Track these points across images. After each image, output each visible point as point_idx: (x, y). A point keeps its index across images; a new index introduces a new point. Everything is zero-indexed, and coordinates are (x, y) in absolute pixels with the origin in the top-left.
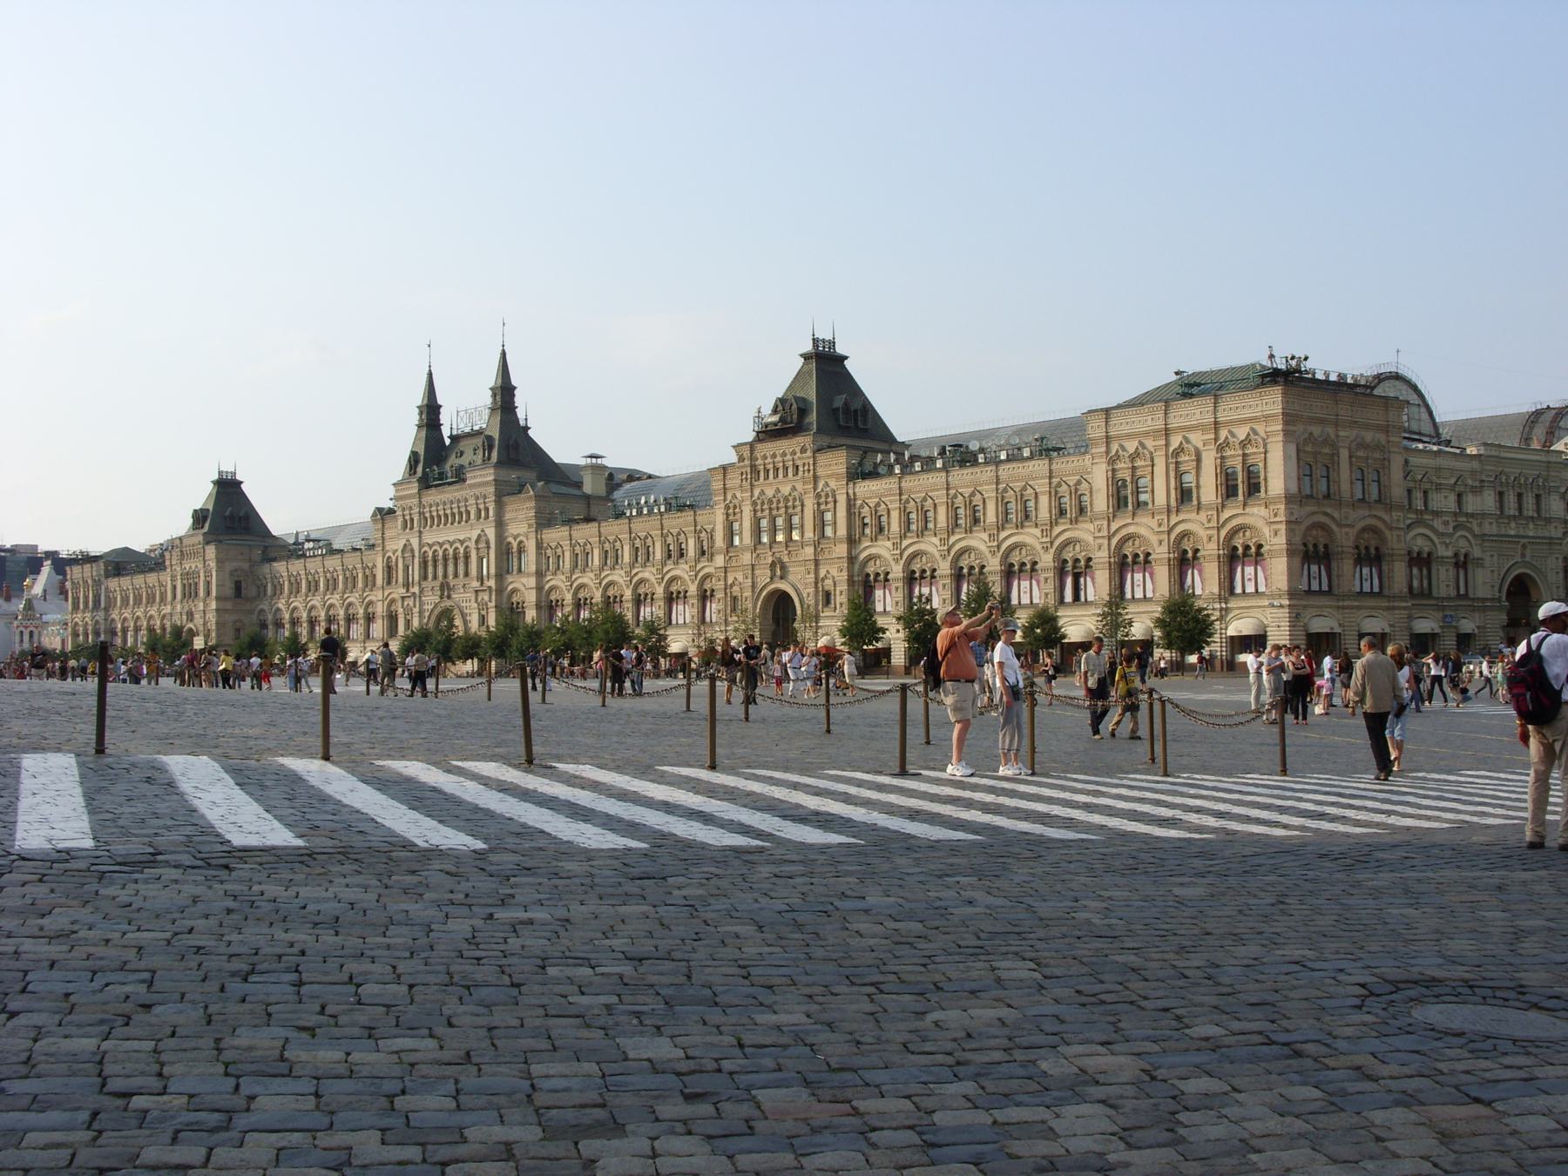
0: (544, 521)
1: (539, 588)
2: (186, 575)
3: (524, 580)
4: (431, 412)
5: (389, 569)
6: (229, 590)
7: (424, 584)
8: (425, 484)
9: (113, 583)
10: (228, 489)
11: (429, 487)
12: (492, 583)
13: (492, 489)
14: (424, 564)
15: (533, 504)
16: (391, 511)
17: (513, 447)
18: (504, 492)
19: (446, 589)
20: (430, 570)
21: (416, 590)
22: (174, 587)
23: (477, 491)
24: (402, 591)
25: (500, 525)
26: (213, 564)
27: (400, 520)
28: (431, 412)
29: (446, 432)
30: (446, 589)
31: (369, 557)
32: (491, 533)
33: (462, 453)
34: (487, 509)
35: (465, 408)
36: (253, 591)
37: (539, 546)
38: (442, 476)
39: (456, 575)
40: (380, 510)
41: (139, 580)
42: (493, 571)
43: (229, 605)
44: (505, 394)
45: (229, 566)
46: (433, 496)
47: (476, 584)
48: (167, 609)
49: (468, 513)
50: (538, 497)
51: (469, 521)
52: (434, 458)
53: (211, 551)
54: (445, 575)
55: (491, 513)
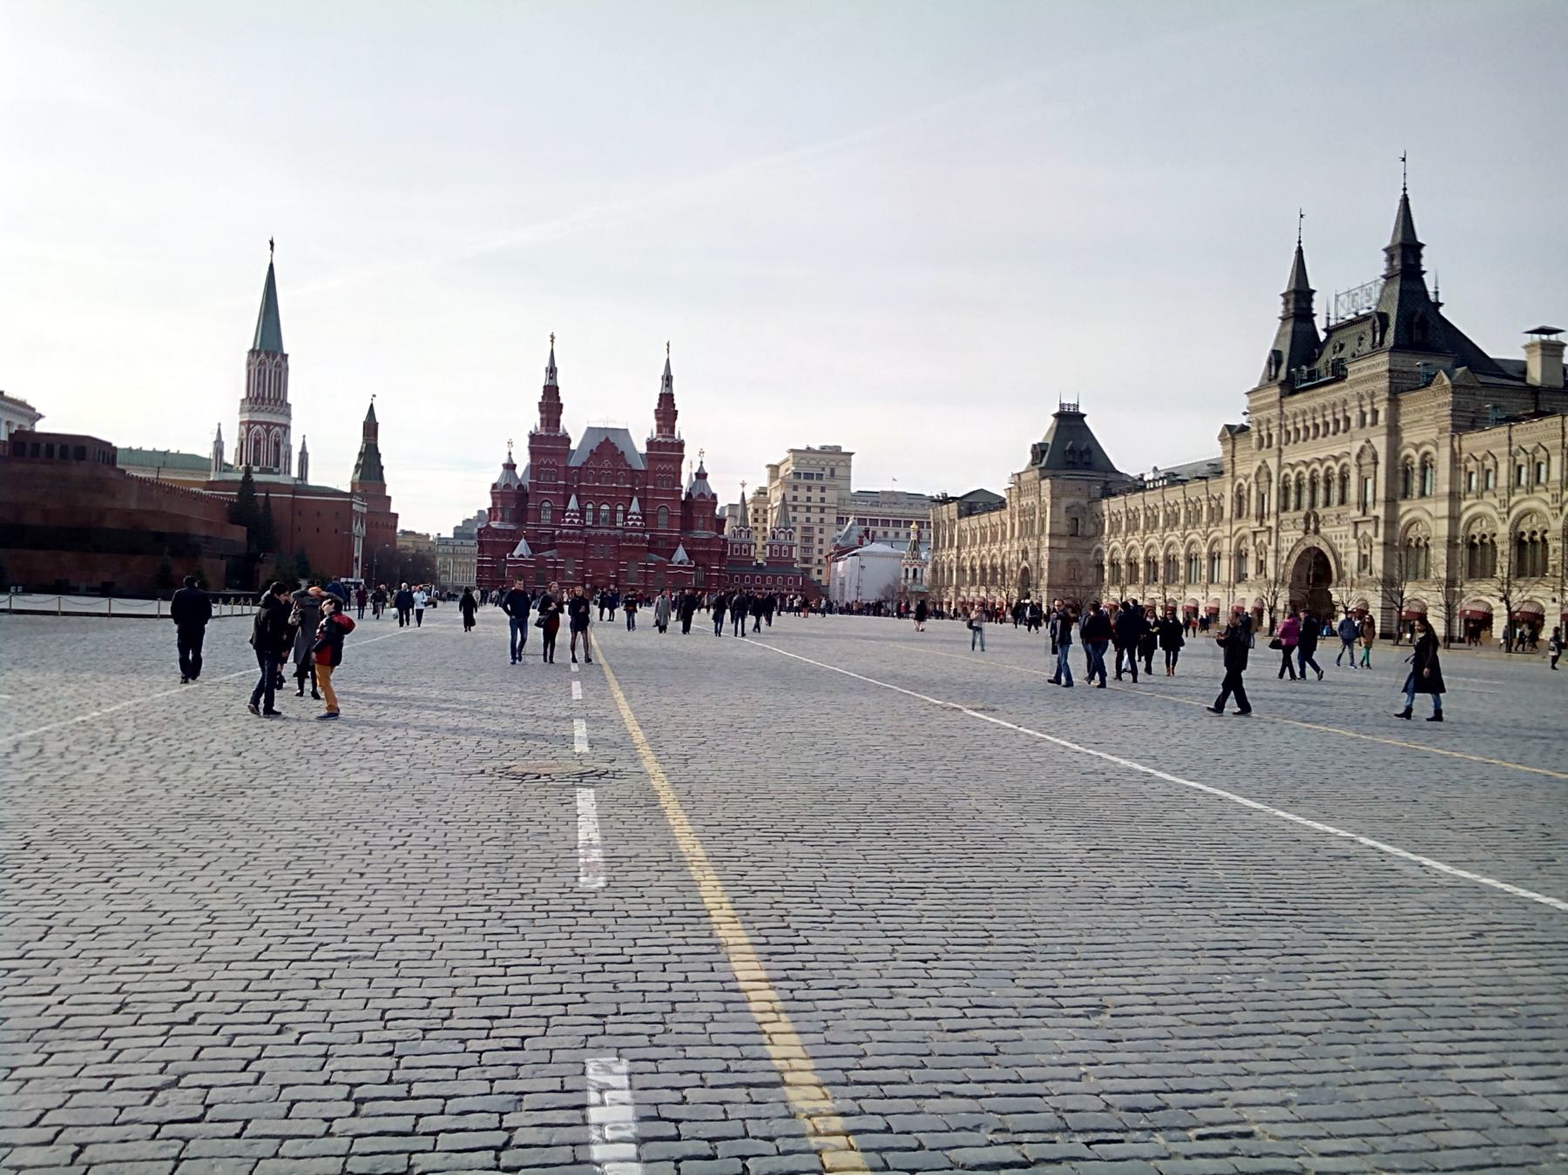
0: (1466, 420)
1: (1454, 518)
2: (1023, 512)
3: (1430, 507)
4: (1300, 298)
5: (1239, 498)
6: (1063, 528)
7: (1283, 516)
8: (1290, 388)
9: (964, 523)
10: (1070, 422)
11: (1294, 392)
12: (1380, 511)
13: (1384, 384)
14: (1284, 490)
15: (1449, 398)
16: (1244, 429)
17: (1416, 327)
18: (1400, 385)
19: (1312, 523)
20: (1293, 497)
21: (1272, 522)
22: (1013, 525)
23: (1361, 389)
24: (1255, 524)
25: (1394, 431)
26: (1048, 500)
27: (1255, 436)
28: (1300, 298)
29: (1320, 324)
30: (1312, 523)
31: (1215, 486)
32: (1380, 444)
33: (1342, 346)
34: (1375, 413)
35: (1350, 284)
36: (1091, 529)
37: (1455, 458)
38: (1312, 375)
39: (1327, 503)
40: (1229, 428)
41: (984, 519)
42: (1381, 494)
43: (1063, 544)
44: (1406, 254)
45: (1065, 502)
46: (1298, 403)
47: (1355, 513)
48: (1007, 548)
49: (1348, 420)
50: (1456, 388)
51: (1348, 430)
52: (1304, 357)
53: (1046, 484)
54: (1313, 504)
55: (1382, 416)
